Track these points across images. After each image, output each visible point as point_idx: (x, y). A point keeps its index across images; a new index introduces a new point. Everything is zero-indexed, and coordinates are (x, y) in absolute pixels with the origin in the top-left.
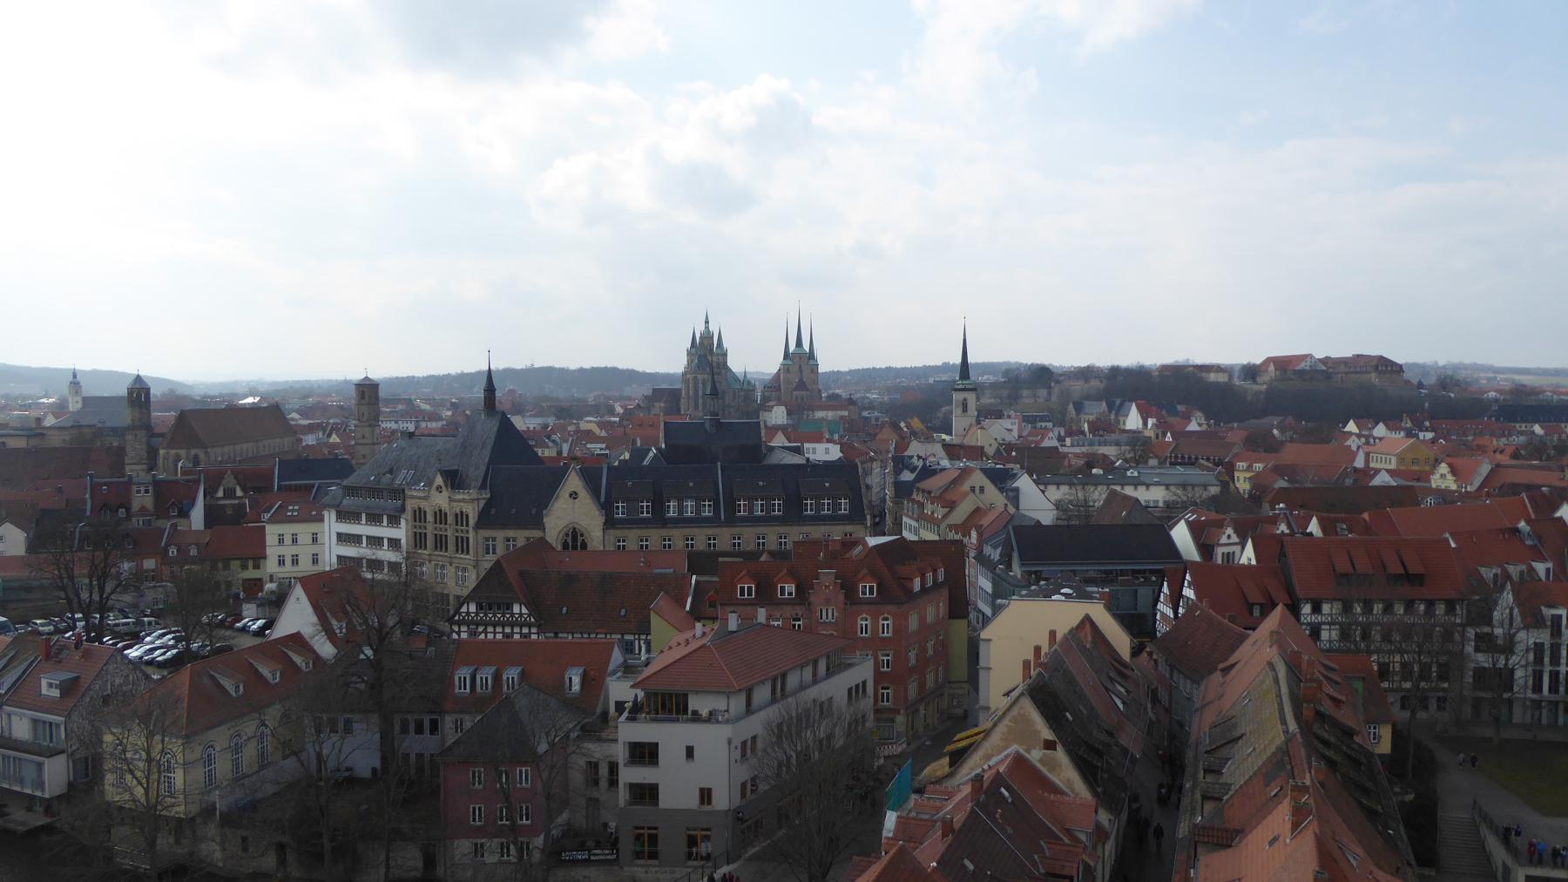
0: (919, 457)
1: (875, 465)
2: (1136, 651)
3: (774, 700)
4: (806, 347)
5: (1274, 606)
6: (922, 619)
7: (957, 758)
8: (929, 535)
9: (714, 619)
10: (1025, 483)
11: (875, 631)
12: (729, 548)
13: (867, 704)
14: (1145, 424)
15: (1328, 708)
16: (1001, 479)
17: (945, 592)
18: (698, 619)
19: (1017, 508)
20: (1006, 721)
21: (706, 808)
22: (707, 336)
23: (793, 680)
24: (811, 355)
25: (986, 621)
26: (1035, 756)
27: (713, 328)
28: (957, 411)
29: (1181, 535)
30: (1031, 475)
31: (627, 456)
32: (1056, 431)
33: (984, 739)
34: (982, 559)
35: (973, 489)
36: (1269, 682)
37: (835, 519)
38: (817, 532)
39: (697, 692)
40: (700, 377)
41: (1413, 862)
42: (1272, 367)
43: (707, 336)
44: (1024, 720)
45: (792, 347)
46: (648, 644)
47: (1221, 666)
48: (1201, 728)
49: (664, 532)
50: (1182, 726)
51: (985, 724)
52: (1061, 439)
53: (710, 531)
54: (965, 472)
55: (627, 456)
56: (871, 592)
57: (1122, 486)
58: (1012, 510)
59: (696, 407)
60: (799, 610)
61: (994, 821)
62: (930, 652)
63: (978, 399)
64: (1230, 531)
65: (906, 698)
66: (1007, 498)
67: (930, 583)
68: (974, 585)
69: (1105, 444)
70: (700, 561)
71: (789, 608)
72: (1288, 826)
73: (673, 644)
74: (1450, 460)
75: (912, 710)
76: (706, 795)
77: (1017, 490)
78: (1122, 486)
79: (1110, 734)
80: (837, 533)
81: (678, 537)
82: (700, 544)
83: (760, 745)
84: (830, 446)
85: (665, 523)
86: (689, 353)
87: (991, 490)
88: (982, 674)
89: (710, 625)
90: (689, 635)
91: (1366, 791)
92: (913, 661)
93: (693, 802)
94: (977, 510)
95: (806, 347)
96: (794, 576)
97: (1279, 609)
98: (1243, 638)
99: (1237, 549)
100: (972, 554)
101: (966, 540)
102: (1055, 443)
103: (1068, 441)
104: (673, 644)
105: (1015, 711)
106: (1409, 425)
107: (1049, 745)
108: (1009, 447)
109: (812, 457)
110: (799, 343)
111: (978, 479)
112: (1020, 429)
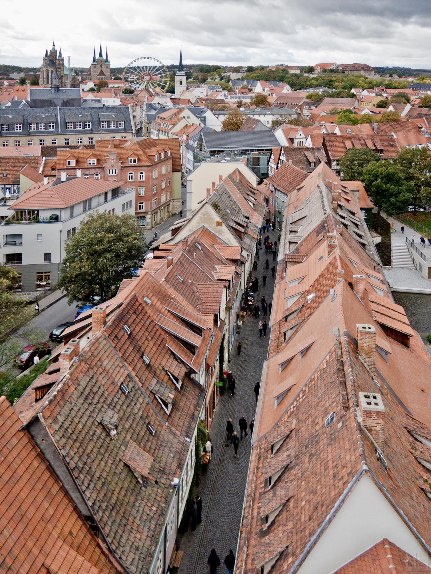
0: (159, 104)
1: (138, 107)
2: (260, 183)
3: (85, 210)
4: (104, 57)
5: (321, 162)
6: (160, 173)
7: (175, 231)
8: (162, 136)
9: (54, 176)
10: (209, 114)
11: (136, 179)
12: (63, 144)
13: (132, 212)
14: (264, 90)
15: (343, 203)
16: (198, 112)
17: (171, 161)
18: (46, 176)
19: (205, 124)
20: (199, 215)
21: (47, 262)
22: (54, 52)
23: (94, 203)
24: (107, 61)
25: (189, 172)
26: (212, 228)
27: (57, 48)
28: (177, 85)
29: (280, 135)
30: (212, 111)
31: (10, 104)
32: (223, 92)
33: (188, 223)
34: (188, 147)
35: (184, 117)
36: (318, 194)
37: (117, 131)
38: (107, 137)
39: (44, 210)
40: (50, 70)
41: (381, 264)
42: (319, 68)
43: (54, 52)
44: (207, 214)
45: (97, 57)
46: (18, 188)
47: (297, 188)
48: (289, 216)
49: (29, 138)
50: (280, 213)
51: (189, 216)
52: (225, 96)
53: (53, 137)
54: (181, 110)
55: (10, 104)
56: (135, 161)
57: (253, 115)
58: (202, 125)
59: (48, 83)
60: (98, 171)
61: (193, 258)
62: (163, 187)
63: (187, 79)
64: (301, 133)
65: (151, 208)
66: (201, 121)
67: (163, 157)
68: (185, 157)
69: (246, 98)
70: (47, 151)
71: (94, 170)
72: (326, 252)
73: (32, 188)
74: (394, 104)
75: (154, 213)
76: (47, 257)
77: (205, 117)
78: (253, 115)
79: (248, 218)
80: (118, 137)
81: (36, 140)
82: (48, 142)
83: (77, 231)
84: (116, 99)
85: (29, 134)
86: (44, 59)
87: (192, 116)
88: (188, 195)
89: (52, 178)
90: (40, 184)
91: (360, 236)
92: (155, 191)
93: (41, 260)
94: (186, 126)
95: (104, 57)
96: (94, 155)
97: (323, 164)
98: (306, 176)
99: (304, 140)
100: (184, 144)
101: (180, 139)
102: (222, 98)
103: (229, 97)
104: (32, 188)
105: (203, 210)
106: (377, 91)
107: (219, 224)
108: (201, 99)
109: (106, 104)
110: (101, 55)
111: (187, 112)
112: (207, 92)
